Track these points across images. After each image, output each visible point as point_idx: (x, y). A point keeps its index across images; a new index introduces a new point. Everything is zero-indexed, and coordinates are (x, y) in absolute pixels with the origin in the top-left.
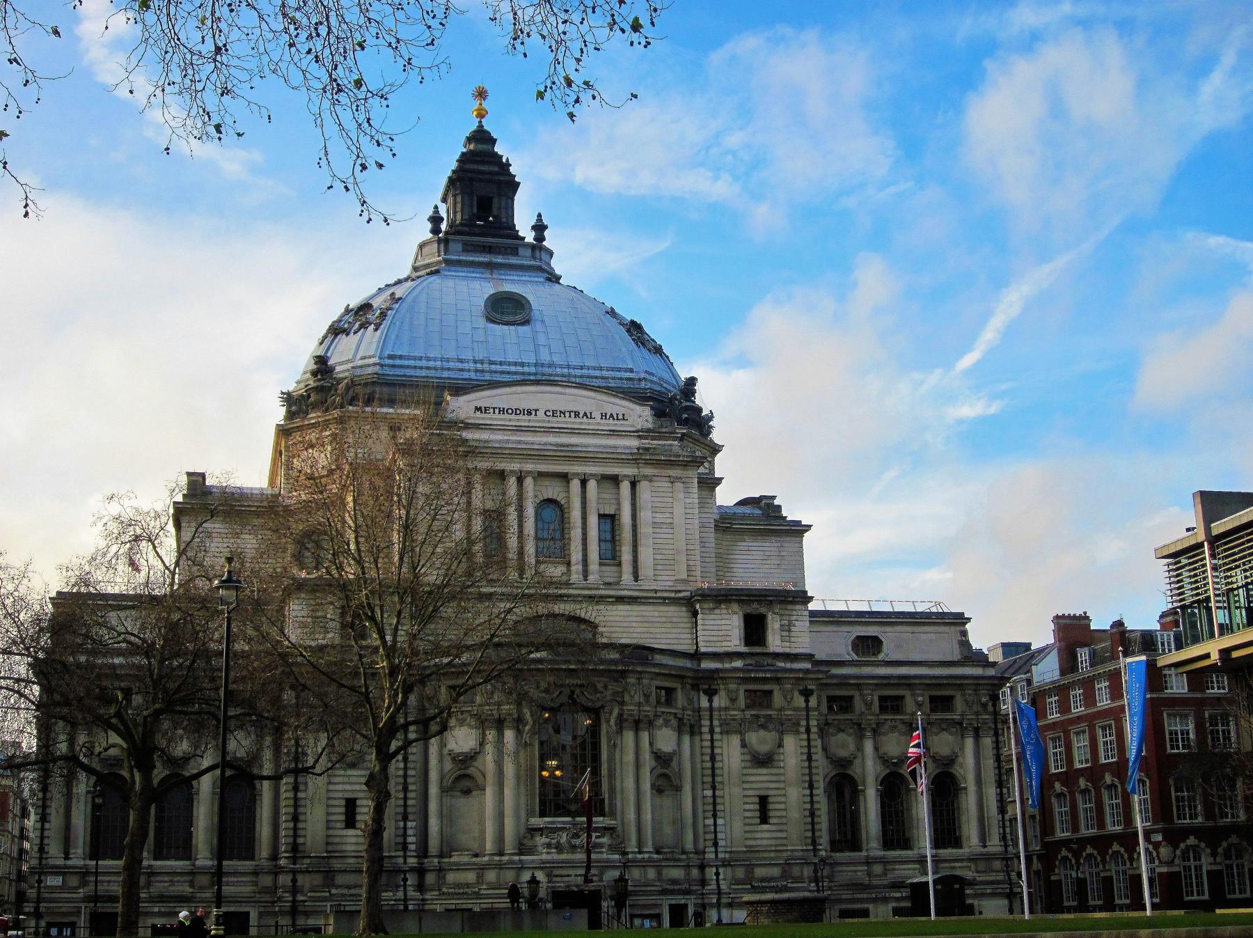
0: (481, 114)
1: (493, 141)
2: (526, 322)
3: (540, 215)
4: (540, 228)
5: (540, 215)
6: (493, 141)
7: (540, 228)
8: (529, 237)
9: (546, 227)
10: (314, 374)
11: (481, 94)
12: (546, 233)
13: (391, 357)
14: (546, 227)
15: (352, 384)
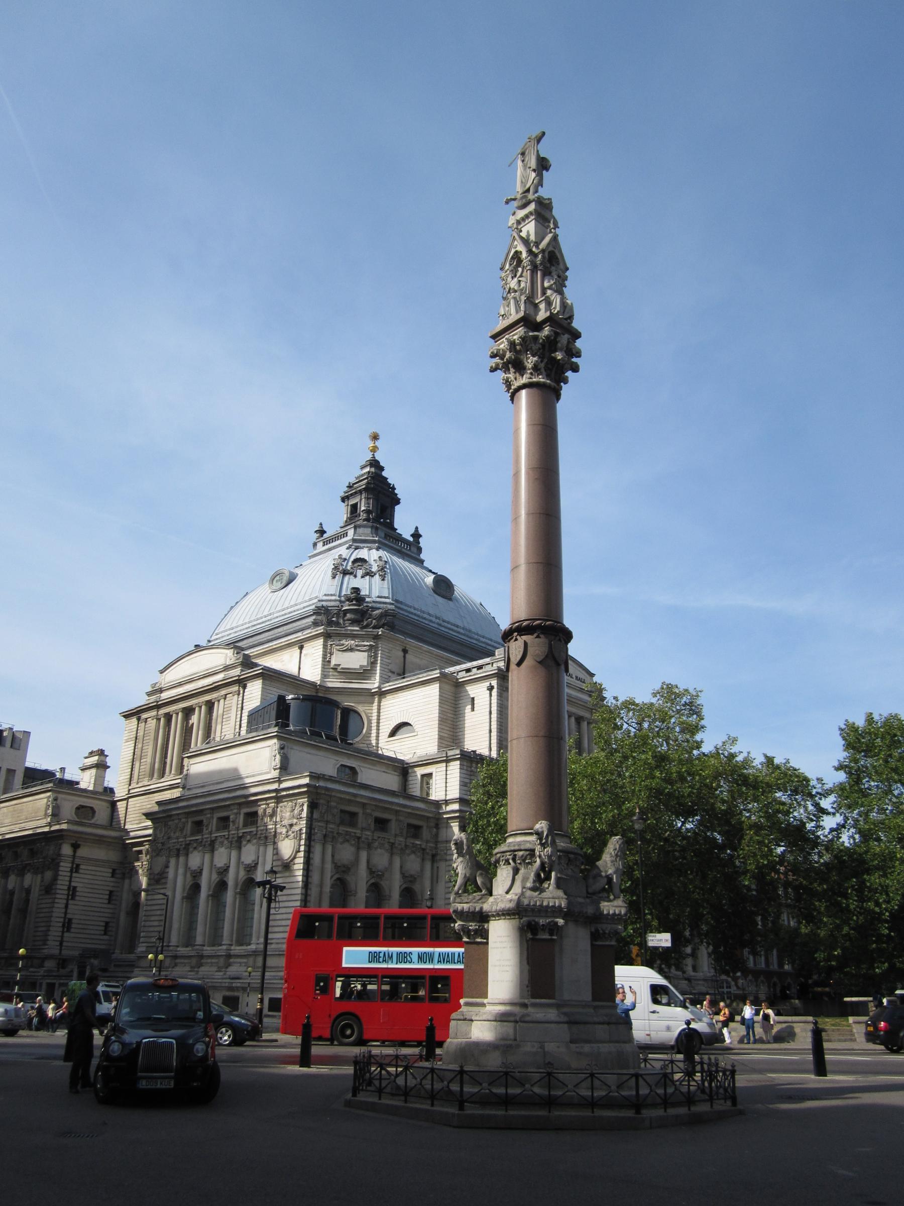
0: (374, 450)
1: (382, 469)
2: (450, 599)
3: (417, 528)
4: (417, 535)
5: (417, 528)
6: (382, 469)
7: (417, 535)
8: (411, 539)
9: (420, 536)
10: (349, 599)
11: (375, 437)
12: (421, 540)
13: (397, 601)
14: (420, 536)
15: (386, 614)
